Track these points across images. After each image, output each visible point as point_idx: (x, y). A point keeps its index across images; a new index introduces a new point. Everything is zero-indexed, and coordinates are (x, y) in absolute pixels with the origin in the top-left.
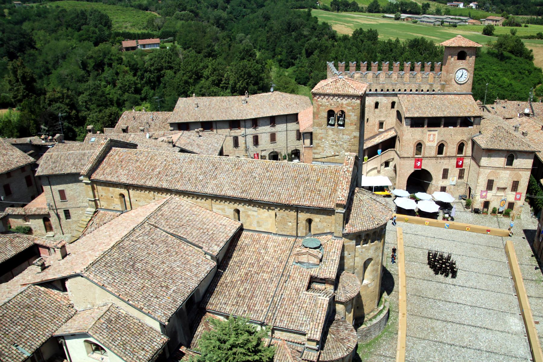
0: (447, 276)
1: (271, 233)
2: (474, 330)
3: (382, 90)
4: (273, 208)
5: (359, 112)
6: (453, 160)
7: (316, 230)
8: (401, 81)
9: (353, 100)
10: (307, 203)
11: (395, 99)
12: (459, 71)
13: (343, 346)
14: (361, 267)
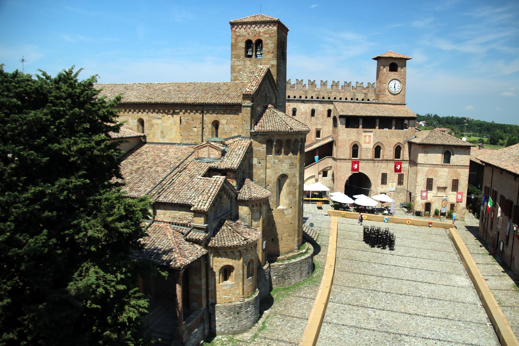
0: (384, 248)
1: (175, 144)
2: (415, 283)
3: (318, 98)
4: (178, 111)
5: (276, 39)
6: (390, 164)
7: (223, 134)
8: (336, 89)
9: (270, 27)
10: (213, 101)
11: (331, 107)
12: (391, 82)
13: (241, 236)
14: (274, 182)
